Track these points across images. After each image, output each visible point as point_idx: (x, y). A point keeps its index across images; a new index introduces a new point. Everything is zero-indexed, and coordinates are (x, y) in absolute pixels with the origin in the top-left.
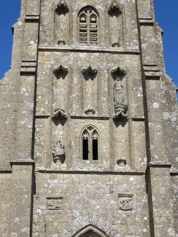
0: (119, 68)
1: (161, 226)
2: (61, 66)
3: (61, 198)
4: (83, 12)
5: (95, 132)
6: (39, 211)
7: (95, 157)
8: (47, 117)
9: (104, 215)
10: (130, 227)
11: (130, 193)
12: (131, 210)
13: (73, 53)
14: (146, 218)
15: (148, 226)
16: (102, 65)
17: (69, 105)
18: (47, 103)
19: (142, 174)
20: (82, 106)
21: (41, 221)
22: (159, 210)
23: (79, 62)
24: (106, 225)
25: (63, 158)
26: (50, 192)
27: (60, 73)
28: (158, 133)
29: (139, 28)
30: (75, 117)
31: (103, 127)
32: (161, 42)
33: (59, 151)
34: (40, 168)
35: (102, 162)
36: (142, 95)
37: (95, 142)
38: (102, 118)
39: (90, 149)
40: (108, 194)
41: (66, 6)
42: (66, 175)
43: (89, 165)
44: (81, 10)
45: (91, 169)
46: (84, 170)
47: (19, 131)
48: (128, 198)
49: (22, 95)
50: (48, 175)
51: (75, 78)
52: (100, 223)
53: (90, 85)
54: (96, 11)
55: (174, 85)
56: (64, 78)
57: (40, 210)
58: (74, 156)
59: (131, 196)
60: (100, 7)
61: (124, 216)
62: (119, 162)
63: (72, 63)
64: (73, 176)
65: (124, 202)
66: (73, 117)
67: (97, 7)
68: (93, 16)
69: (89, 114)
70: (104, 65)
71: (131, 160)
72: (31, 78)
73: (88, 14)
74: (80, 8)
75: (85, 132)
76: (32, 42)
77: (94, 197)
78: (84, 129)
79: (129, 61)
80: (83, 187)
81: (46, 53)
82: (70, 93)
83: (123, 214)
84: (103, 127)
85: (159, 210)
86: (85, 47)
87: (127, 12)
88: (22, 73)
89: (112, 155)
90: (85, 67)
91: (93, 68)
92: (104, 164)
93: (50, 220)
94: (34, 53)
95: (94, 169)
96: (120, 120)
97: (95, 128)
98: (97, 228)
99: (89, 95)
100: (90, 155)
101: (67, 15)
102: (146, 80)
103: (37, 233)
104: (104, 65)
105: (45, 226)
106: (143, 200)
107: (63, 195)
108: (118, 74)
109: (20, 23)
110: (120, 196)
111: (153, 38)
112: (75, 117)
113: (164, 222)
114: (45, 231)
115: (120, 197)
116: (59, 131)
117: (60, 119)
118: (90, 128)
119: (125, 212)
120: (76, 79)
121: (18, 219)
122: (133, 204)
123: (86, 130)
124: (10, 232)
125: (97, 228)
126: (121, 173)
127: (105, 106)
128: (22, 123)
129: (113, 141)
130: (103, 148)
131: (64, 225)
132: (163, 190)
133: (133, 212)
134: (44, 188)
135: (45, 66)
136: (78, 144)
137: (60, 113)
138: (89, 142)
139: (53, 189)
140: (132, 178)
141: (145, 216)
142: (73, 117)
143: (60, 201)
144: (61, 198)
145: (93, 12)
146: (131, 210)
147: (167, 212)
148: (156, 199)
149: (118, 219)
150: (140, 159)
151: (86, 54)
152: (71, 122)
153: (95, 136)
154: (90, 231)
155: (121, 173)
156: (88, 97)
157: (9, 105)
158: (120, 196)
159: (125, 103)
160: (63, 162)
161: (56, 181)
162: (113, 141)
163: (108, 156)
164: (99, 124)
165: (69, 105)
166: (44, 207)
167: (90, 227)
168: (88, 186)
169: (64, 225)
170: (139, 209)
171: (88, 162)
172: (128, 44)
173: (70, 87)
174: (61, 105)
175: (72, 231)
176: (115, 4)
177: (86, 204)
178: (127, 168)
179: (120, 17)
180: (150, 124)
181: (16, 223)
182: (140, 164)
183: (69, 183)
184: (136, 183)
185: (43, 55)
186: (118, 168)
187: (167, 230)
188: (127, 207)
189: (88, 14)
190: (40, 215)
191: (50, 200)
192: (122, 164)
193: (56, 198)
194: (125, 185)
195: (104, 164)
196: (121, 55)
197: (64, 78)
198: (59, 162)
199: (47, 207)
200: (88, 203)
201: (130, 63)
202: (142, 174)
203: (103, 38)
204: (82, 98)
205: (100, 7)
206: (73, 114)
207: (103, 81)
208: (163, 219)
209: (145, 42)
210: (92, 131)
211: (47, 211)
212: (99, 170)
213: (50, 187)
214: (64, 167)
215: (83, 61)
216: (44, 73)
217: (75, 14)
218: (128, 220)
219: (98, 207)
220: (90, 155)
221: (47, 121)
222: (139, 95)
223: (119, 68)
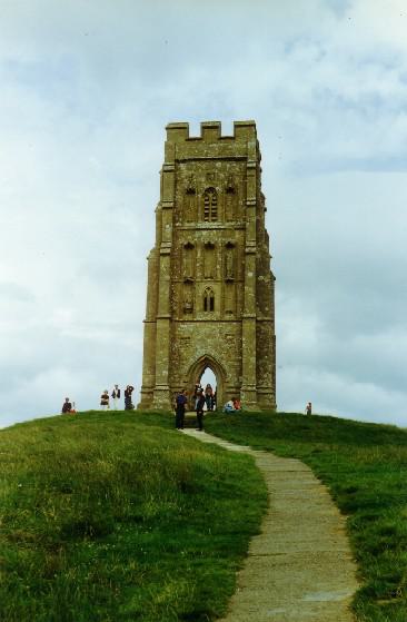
7: (212, 309)
33: (188, 306)
37: (212, 300)
39: (209, 304)
47: (161, 296)
53: (210, 257)
58: (198, 309)
62: (227, 312)
72: (167, 258)
73: (211, 195)
77: (208, 337)
82: (195, 263)
92: (217, 314)
100: (209, 307)
118: (209, 288)
127: (219, 276)
129: (223, 298)
130: (217, 303)
215: (204, 237)
217: (200, 196)
220: (209, 307)
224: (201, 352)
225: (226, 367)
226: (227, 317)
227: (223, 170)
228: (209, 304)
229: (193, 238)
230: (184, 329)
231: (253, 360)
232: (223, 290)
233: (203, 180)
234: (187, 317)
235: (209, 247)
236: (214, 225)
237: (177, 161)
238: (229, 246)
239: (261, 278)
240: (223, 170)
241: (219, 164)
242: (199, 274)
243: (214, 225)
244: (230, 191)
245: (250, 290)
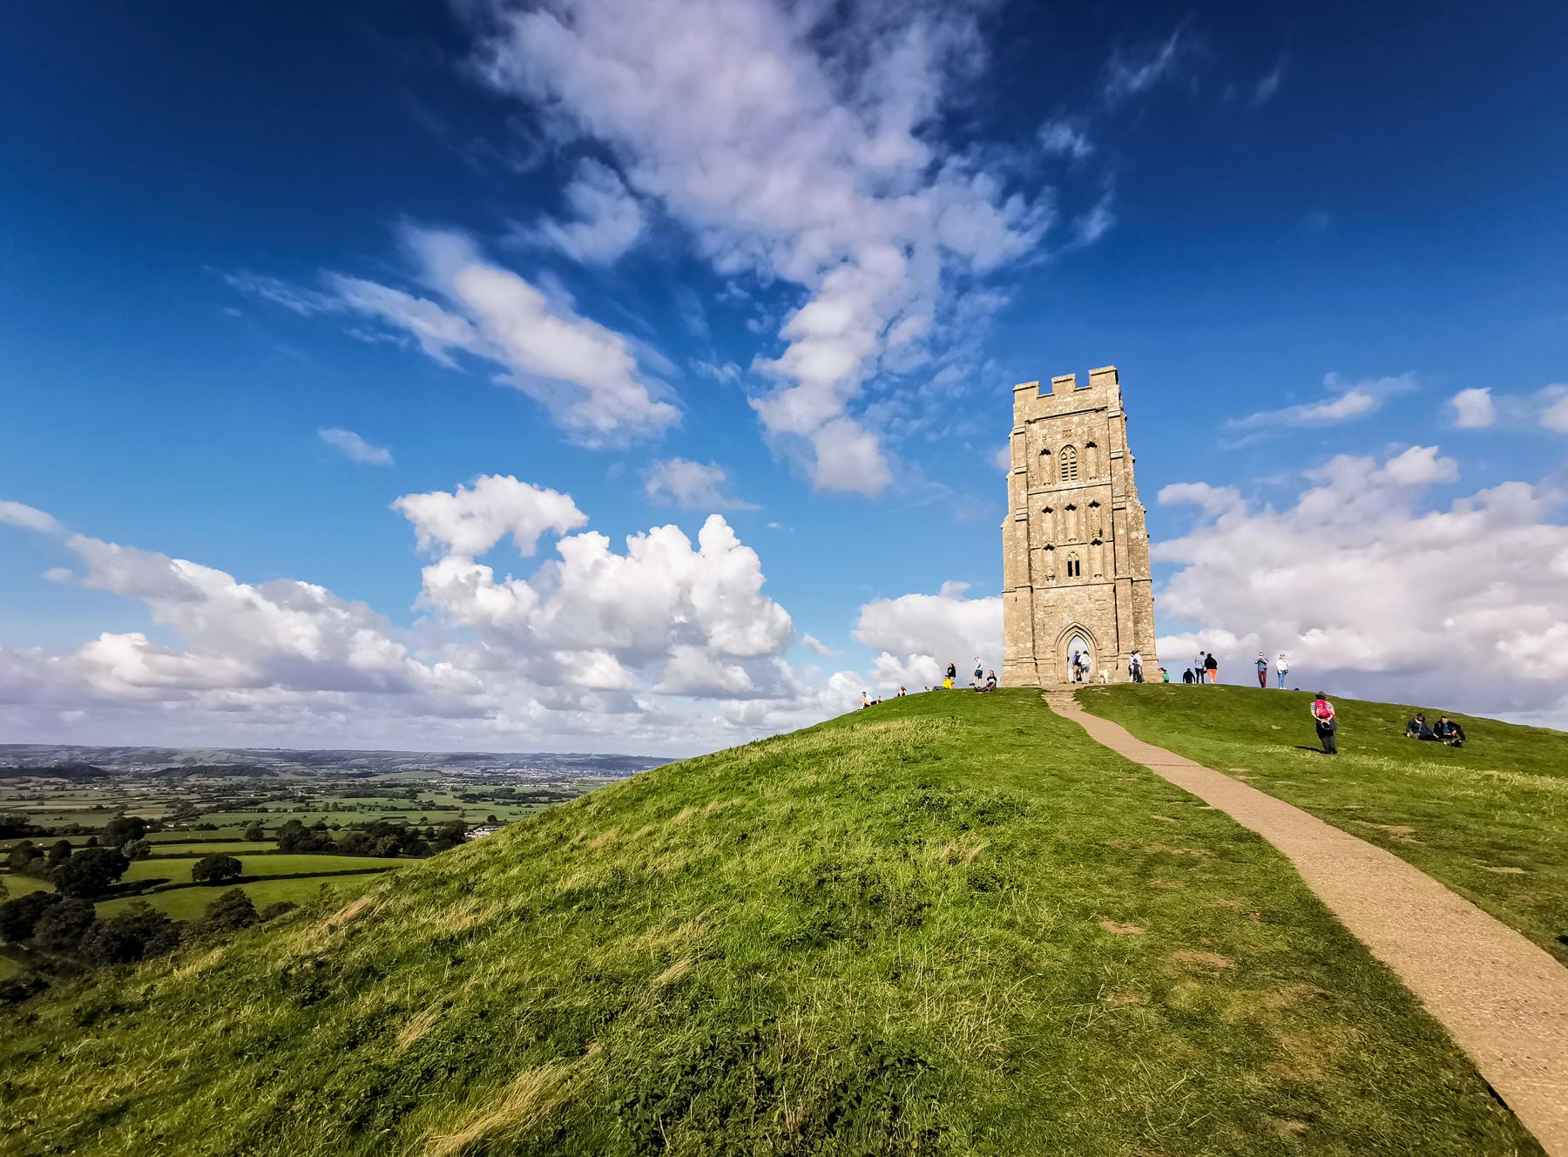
17: (1056, 537)
31: (1082, 552)
33: (1050, 573)
39: (1074, 569)
43: (1074, 580)
57: (1039, 615)
69: (1070, 542)
70: (1082, 501)
86: (1065, 485)
87: (1102, 444)
89: (1090, 571)
92: (1084, 578)
96: (1096, 542)
104: (1082, 501)
130: (1083, 567)
152: (1057, 550)
165: (1056, 537)
173: (1055, 522)
177: (1071, 609)
178: (1101, 580)
186: (1095, 581)
215: (1066, 498)
224: (1068, 620)
225: (1098, 634)
226: (1095, 581)
227: (1080, 424)
228: (1074, 569)
229: (1050, 501)
231: (1131, 624)
232: (1089, 551)
233: (1059, 436)
234: (1053, 583)
236: (1074, 484)
237: (1029, 422)
238: (1095, 504)
239: (1134, 535)
240: (1080, 424)
241: (1076, 419)
242: (1061, 537)
243: (1074, 484)
244: (1091, 445)
245: (1122, 550)
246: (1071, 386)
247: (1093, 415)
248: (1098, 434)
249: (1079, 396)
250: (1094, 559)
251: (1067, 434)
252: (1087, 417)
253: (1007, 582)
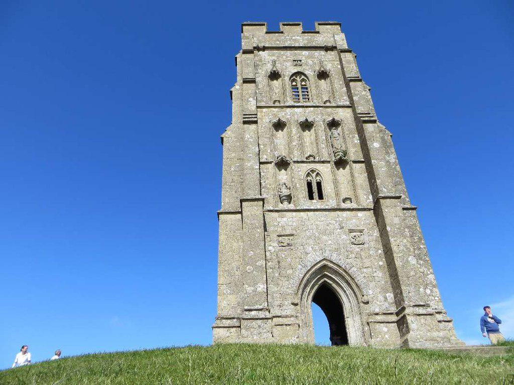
0: (334, 119)
1: (401, 254)
2: (279, 120)
3: (292, 235)
4: (294, 77)
5: (318, 174)
6: (270, 248)
7: (321, 197)
8: (271, 163)
9: (337, 250)
10: (365, 261)
11: (361, 228)
12: (363, 244)
13: (289, 109)
14: (380, 251)
15: (384, 259)
16: (317, 117)
17: (290, 152)
18: (269, 151)
19: (370, 210)
20: (303, 152)
21: (274, 257)
22: (395, 239)
23: (296, 116)
24: (340, 260)
25: (289, 198)
26: (280, 229)
27: (279, 125)
28: (383, 169)
29: (348, 86)
30: (298, 162)
32: (370, 97)
33: (285, 192)
34: (269, 208)
35: (328, 201)
36: (359, 141)
37: (319, 185)
38: (323, 162)
39: (315, 190)
40: (338, 230)
41: (278, 73)
42: (294, 214)
43: (316, 203)
44: (291, 78)
45: (319, 207)
46: (312, 208)
48: (359, 233)
49: (247, 141)
50: (276, 214)
51: (293, 130)
52: (334, 258)
53: (308, 135)
54: (305, 75)
55: (387, 132)
56: (282, 130)
58: (301, 196)
59: (361, 231)
60: (309, 72)
61: (358, 250)
63: (289, 117)
64: (302, 213)
65: (355, 236)
66: (295, 162)
67: (306, 72)
68: (303, 80)
71: (356, 197)
72: (253, 126)
73: (298, 79)
74: (291, 74)
75: (308, 175)
76: (251, 99)
77: (324, 233)
78: (307, 173)
79: (341, 113)
80: (312, 224)
81: (264, 110)
83: (356, 248)
84: (326, 171)
85: (395, 239)
88: (245, 123)
89: (337, 195)
90: (302, 119)
91: (309, 120)
93: (283, 256)
94: (254, 108)
95: (322, 207)
96: (341, 163)
97: (317, 171)
98: (331, 262)
99: (307, 144)
100: (316, 195)
101: (280, 80)
102: (364, 125)
103: (271, 270)
104: (319, 117)
105: (279, 262)
106: (375, 234)
107: (294, 232)
108: (334, 124)
109: (237, 87)
110: (351, 231)
111: (361, 91)
112: (298, 162)
113: (403, 250)
114: (279, 268)
115: (350, 233)
116: (283, 176)
117: (282, 164)
118: (313, 171)
119: (358, 246)
120: (295, 130)
121: (252, 252)
122: (365, 238)
123: (309, 173)
124: (245, 266)
125: (331, 262)
126: (349, 210)
128: (249, 165)
129: (336, 182)
130: (327, 188)
131: (297, 260)
132: (396, 220)
133: (366, 246)
134: (274, 226)
135: (264, 120)
136: (303, 185)
137: (282, 158)
138: (313, 184)
139: (283, 227)
140: (360, 214)
141: (379, 249)
142: (295, 162)
143: (291, 238)
144: (292, 235)
145: (303, 77)
146: (363, 244)
147: (405, 241)
148: (391, 229)
149: (352, 252)
150: (365, 197)
151: (301, 109)
152: (294, 166)
153: (318, 178)
154: (325, 267)
155: (349, 210)
156: (307, 146)
157: (233, 155)
158: (351, 231)
159: (344, 148)
160: (290, 203)
161: (285, 219)
162: (336, 182)
163: (334, 195)
164: (322, 168)
166: (276, 244)
167: (324, 262)
168: (317, 223)
169: (297, 260)
170: (372, 244)
171: (314, 201)
172: (338, 100)
174: (283, 152)
175: (306, 266)
176: (322, 69)
177: (317, 240)
179: (328, 80)
180: (373, 161)
181: (251, 257)
182: (366, 201)
183: (298, 220)
184: (366, 219)
185: (262, 112)
186: (343, 206)
187: (407, 259)
188: (359, 241)
189: (298, 79)
190: (272, 251)
191: (280, 238)
192: (349, 202)
193: (287, 235)
194: (354, 220)
195: (331, 203)
196: (334, 109)
197: (282, 130)
198: (286, 203)
199: (279, 244)
200: (319, 239)
201: (344, 115)
202: (370, 210)
203: (315, 97)
204: (301, 146)
205: (309, 72)
206: (295, 159)
207: (320, 131)
208: (401, 248)
209: (356, 95)
210: (315, 173)
211: (279, 248)
212: (327, 207)
213: (280, 225)
214: (291, 206)
215: (300, 115)
216: (264, 126)
217: (287, 79)
218: (362, 253)
219: (330, 242)
220: (316, 195)
221: (271, 167)
222: (356, 142)
223: (334, 119)
225: (360, 279)
227: (312, 57)
230: (288, 221)
233: (289, 64)
235: (306, 126)
246: (299, 29)
247: (323, 53)
248: (329, 67)
249: (308, 36)
250: (338, 183)
251: (297, 62)
252: (317, 53)
253: (228, 200)
